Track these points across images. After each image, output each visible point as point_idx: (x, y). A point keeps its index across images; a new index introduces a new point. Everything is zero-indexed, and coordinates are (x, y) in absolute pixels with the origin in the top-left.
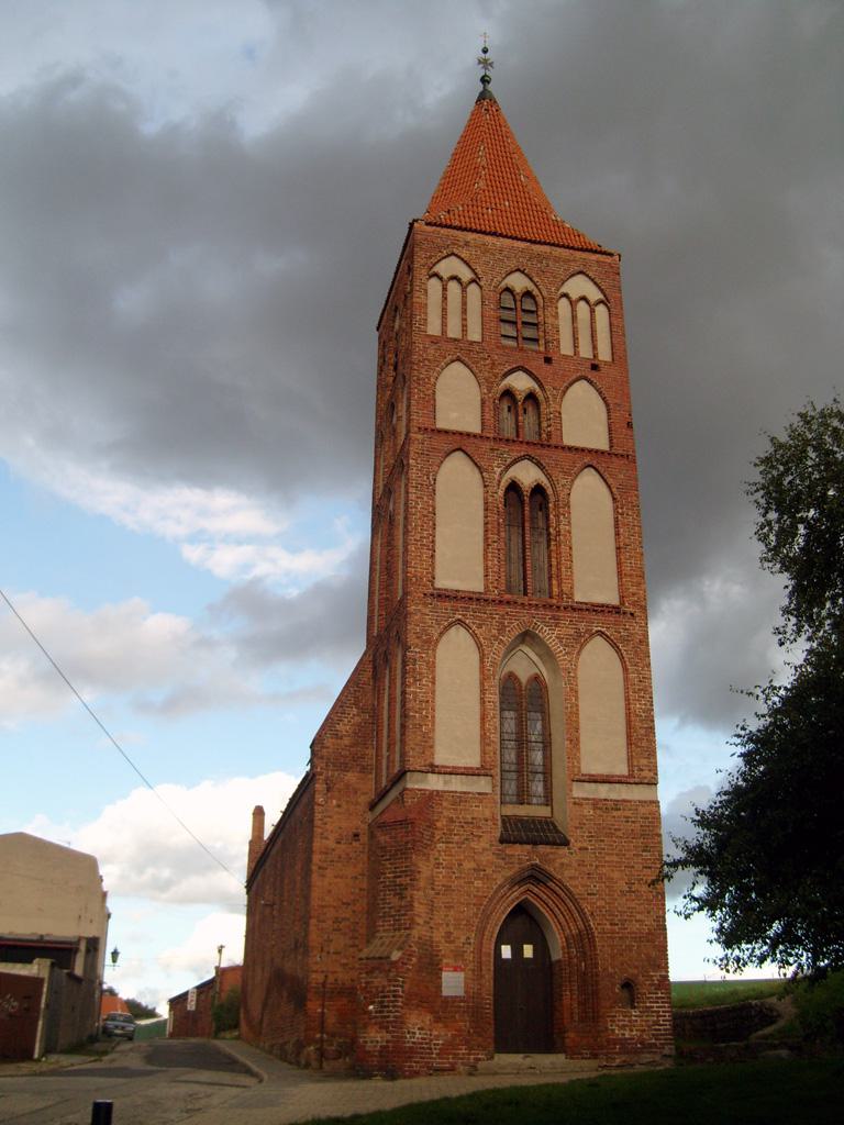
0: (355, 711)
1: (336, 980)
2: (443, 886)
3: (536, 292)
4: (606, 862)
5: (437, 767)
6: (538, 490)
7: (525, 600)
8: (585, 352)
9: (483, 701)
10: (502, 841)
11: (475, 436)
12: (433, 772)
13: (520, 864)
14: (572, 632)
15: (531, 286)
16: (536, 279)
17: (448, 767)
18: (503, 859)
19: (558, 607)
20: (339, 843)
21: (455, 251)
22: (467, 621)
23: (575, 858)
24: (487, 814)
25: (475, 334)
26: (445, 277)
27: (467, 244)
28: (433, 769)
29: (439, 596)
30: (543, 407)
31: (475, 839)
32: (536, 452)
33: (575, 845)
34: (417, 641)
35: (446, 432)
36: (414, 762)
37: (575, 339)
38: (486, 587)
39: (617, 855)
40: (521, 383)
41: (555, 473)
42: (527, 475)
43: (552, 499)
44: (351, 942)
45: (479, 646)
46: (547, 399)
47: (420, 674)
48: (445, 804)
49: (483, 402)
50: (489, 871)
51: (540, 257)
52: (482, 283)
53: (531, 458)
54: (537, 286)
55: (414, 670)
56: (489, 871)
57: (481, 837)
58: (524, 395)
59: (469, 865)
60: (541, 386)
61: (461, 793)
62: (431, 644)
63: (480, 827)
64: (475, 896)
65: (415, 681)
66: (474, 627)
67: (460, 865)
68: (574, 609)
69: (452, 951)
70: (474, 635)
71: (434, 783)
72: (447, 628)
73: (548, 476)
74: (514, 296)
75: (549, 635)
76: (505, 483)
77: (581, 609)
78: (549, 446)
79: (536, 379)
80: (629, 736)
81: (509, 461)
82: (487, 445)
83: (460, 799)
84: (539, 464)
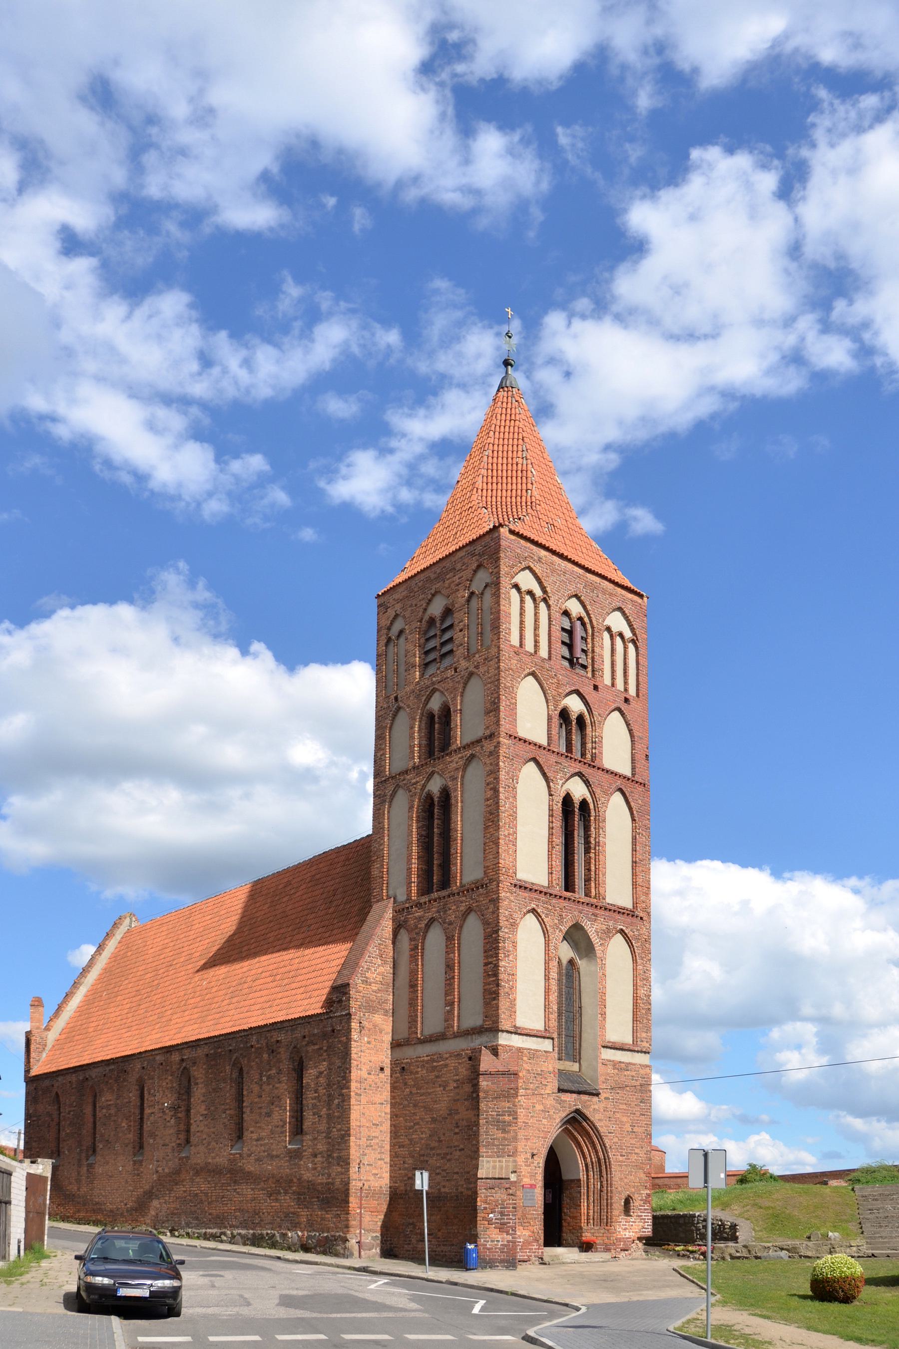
0: (379, 962)
1: (369, 1187)
2: (524, 1122)
4: (620, 1109)
5: (519, 1028)
6: (584, 803)
7: (587, 900)
9: (547, 978)
10: (560, 1090)
12: (516, 1033)
13: (569, 1108)
14: (604, 927)
17: (526, 1029)
18: (560, 1104)
19: (596, 906)
20: (369, 1074)
21: (532, 566)
22: (539, 911)
23: (602, 1105)
24: (551, 1069)
25: (544, 653)
27: (540, 560)
28: (517, 1031)
29: (520, 887)
31: (544, 1087)
32: (586, 771)
33: (602, 1096)
34: (506, 922)
36: (505, 1024)
37: (613, 672)
38: (550, 882)
39: (626, 1104)
40: (575, 705)
41: (598, 791)
42: (578, 790)
43: (593, 813)
44: (379, 1157)
45: (545, 932)
47: (508, 951)
48: (525, 1058)
50: (552, 1113)
52: (551, 603)
53: (580, 775)
55: (505, 947)
56: (552, 1113)
57: (546, 1085)
59: (539, 1107)
61: (534, 1050)
62: (514, 925)
63: (546, 1078)
64: (543, 1131)
65: (505, 957)
66: (543, 916)
67: (534, 1107)
68: (606, 909)
69: (528, 1173)
70: (542, 923)
71: (517, 1041)
72: (525, 914)
73: (592, 793)
74: (570, 619)
75: (592, 929)
76: (563, 794)
77: (610, 910)
78: (594, 767)
79: (586, 703)
80: (635, 1014)
81: (568, 775)
82: (553, 758)
83: (534, 1054)
84: (587, 783)
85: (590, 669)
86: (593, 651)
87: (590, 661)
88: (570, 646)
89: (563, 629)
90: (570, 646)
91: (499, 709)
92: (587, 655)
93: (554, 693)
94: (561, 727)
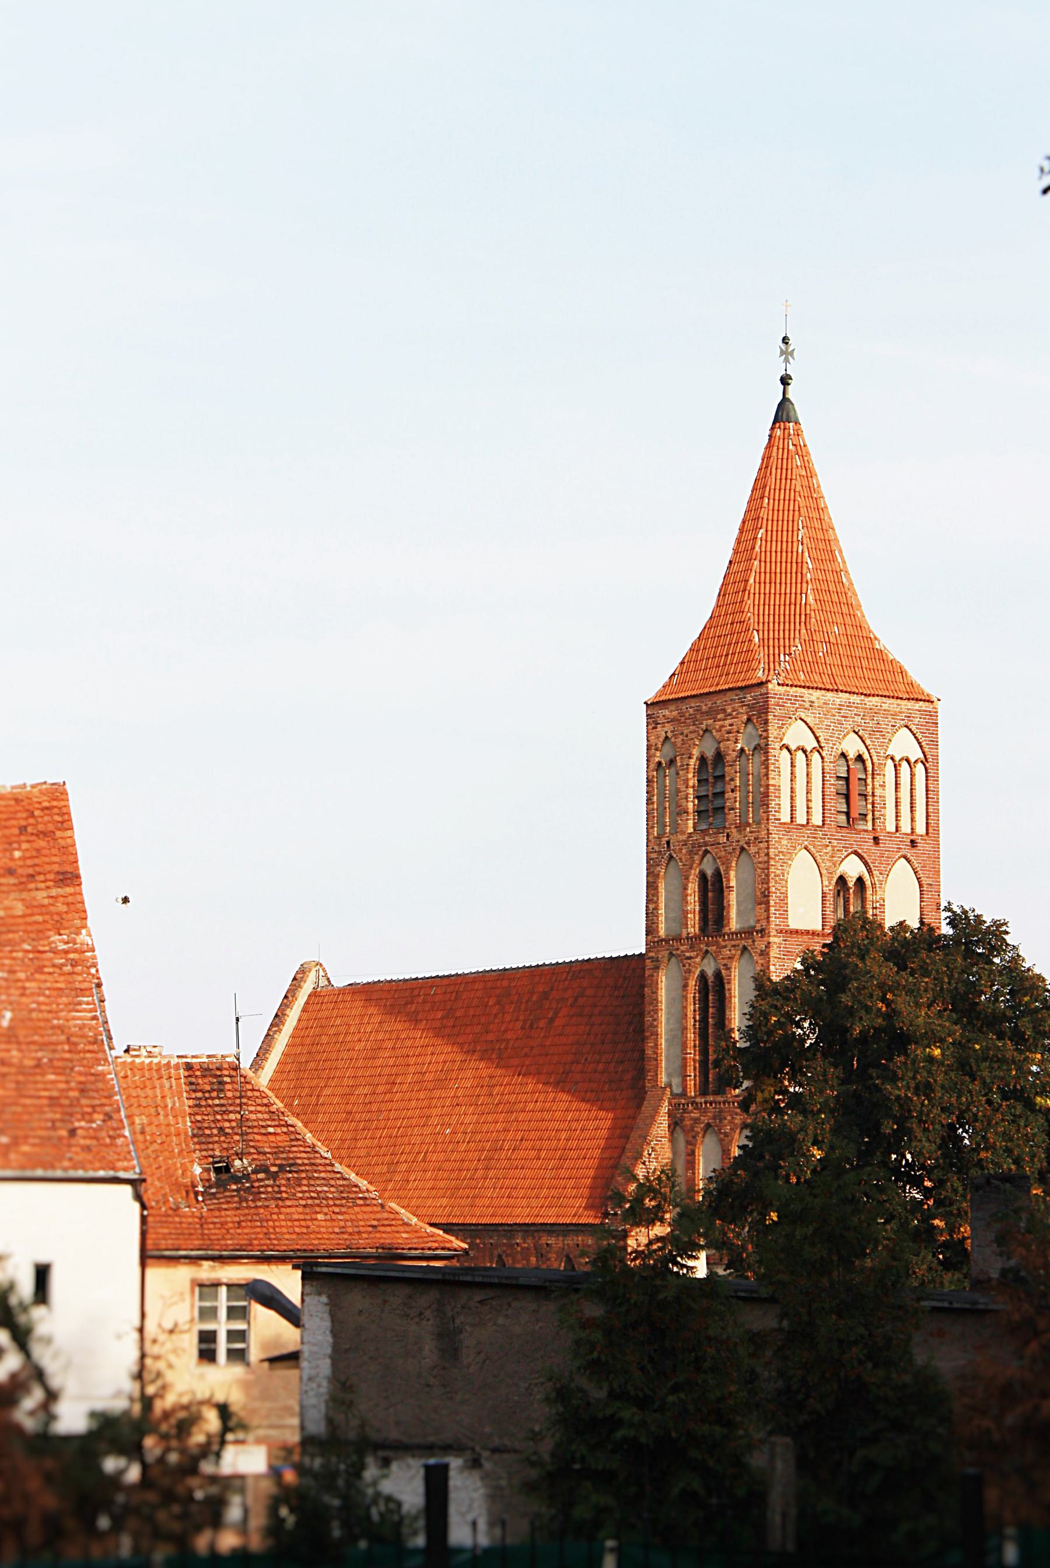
3: (866, 756)
8: (906, 828)
11: (818, 935)
15: (863, 750)
16: (868, 742)
25: (817, 820)
26: (793, 747)
30: (869, 892)
35: (797, 931)
46: (873, 885)
49: (824, 895)
51: (873, 712)
52: (824, 754)
54: (868, 750)
58: (854, 880)
60: (870, 871)
74: (847, 761)
79: (866, 864)
85: (870, 817)
86: (873, 795)
87: (870, 807)
88: (847, 797)
89: (839, 778)
90: (847, 797)
91: (769, 903)
92: (866, 800)
93: (829, 864)
94: (839, 895)
